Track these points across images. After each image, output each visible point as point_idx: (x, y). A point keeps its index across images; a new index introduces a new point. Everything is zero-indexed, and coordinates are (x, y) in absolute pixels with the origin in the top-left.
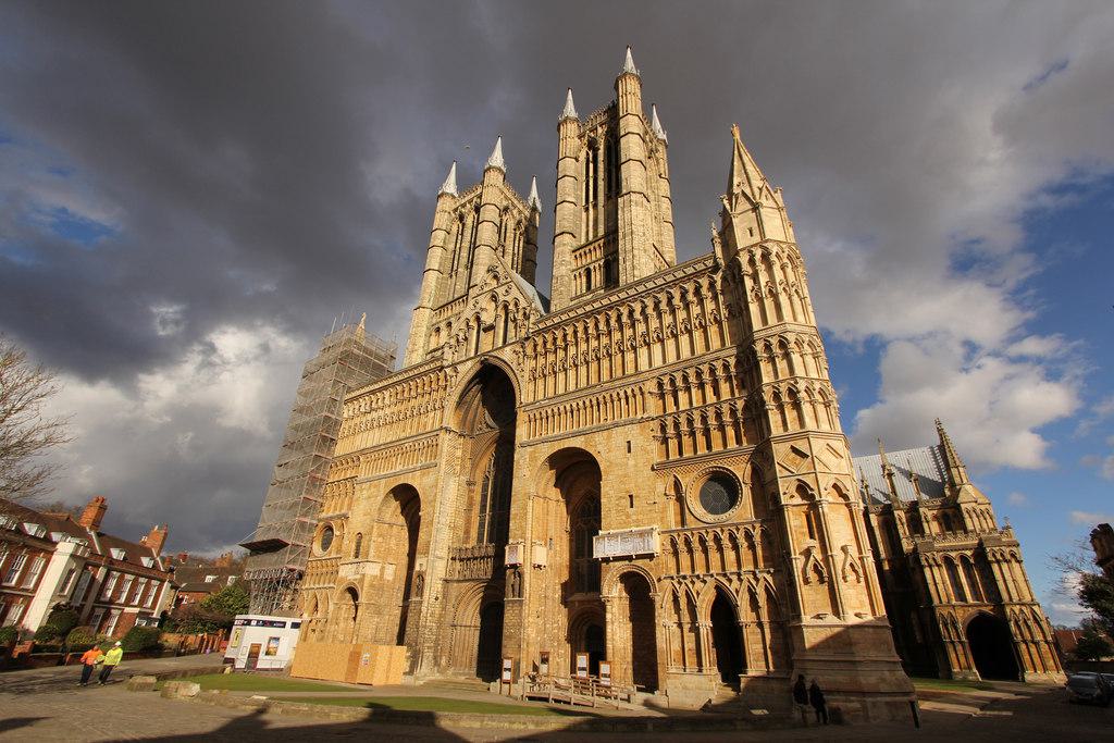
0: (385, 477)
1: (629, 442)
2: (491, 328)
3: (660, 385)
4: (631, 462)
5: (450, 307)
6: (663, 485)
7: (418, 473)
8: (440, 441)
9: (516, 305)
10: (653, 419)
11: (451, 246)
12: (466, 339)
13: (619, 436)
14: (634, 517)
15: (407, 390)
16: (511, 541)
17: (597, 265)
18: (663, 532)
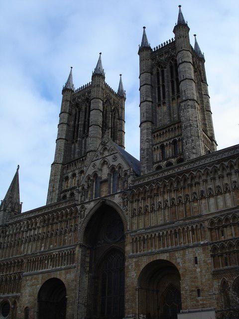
0: (41, 273)
1: (196, 258)
2: (106, 181)
3: (212, 223)
4: (198, 270)
6: (217, 284)
7: (63, 272)
8: (76, 252)
10: (210, 244)
11: (72, 123)
12: (89, 187)
13: (189, 255)
14: (201, 302)
15: (51, 218)
16: (126, 315)
18: (218, 311)
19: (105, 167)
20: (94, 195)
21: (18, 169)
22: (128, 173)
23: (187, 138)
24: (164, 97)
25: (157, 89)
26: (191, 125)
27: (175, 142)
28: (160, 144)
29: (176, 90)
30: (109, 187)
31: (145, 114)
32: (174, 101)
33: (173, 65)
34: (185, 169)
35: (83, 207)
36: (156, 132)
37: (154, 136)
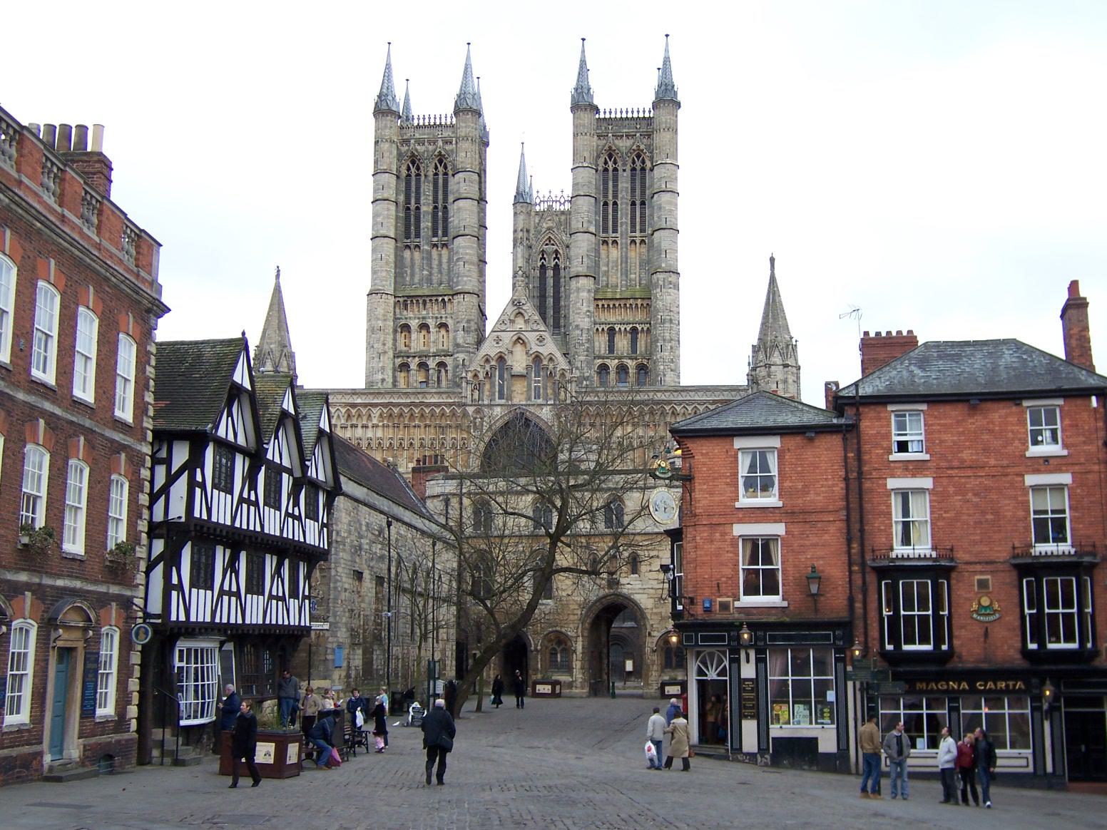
5: (421, 302)
9: (551, 359)
11: (402, 198)
17: (623, 329)
19: (519, 348)
20: (497, 394)
21: (278, 276)
22: (568, 376)
23: (664, 340)
24: (615, 231)
25: (602, 204)
26: (671, 320)
27: (634, 330)
28: (608, 326)
29: (638, 227)
30: (529, 385)
31: (585, 260)
32: (633, 246)
33: (638, 168)
34: (663, 398)
35: (477, 411)
36: (601, 299)
37: (598, 305)
